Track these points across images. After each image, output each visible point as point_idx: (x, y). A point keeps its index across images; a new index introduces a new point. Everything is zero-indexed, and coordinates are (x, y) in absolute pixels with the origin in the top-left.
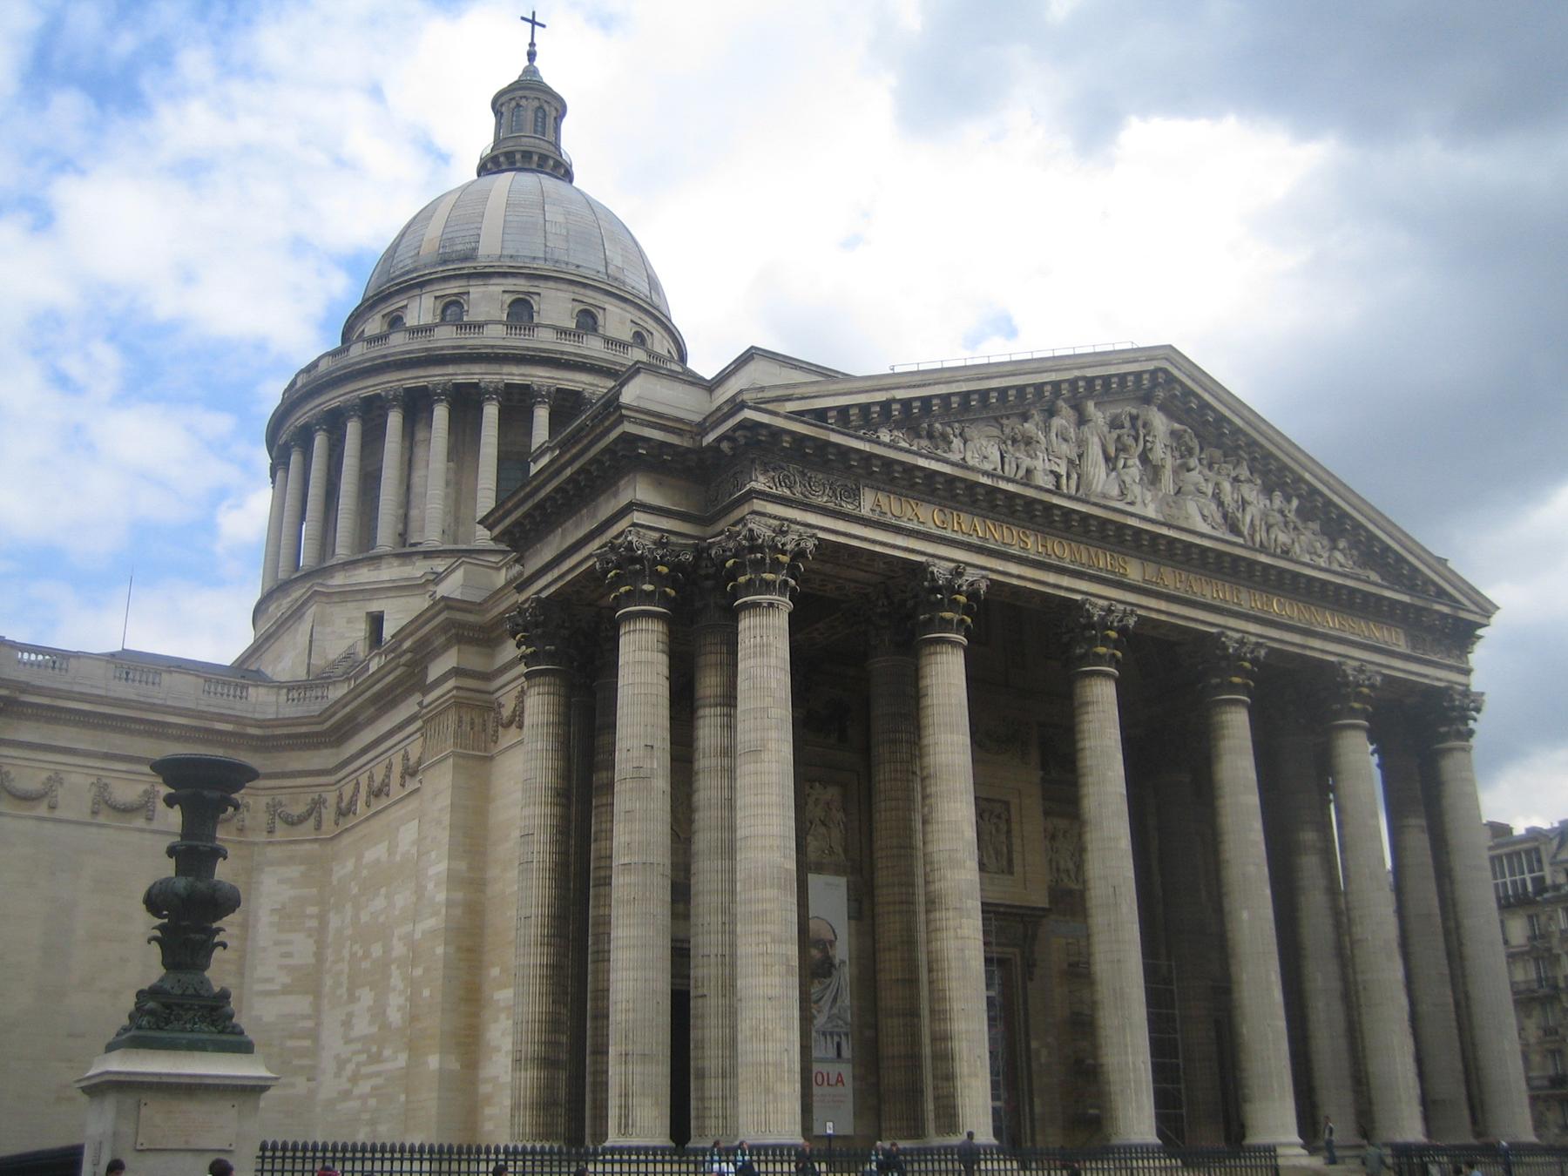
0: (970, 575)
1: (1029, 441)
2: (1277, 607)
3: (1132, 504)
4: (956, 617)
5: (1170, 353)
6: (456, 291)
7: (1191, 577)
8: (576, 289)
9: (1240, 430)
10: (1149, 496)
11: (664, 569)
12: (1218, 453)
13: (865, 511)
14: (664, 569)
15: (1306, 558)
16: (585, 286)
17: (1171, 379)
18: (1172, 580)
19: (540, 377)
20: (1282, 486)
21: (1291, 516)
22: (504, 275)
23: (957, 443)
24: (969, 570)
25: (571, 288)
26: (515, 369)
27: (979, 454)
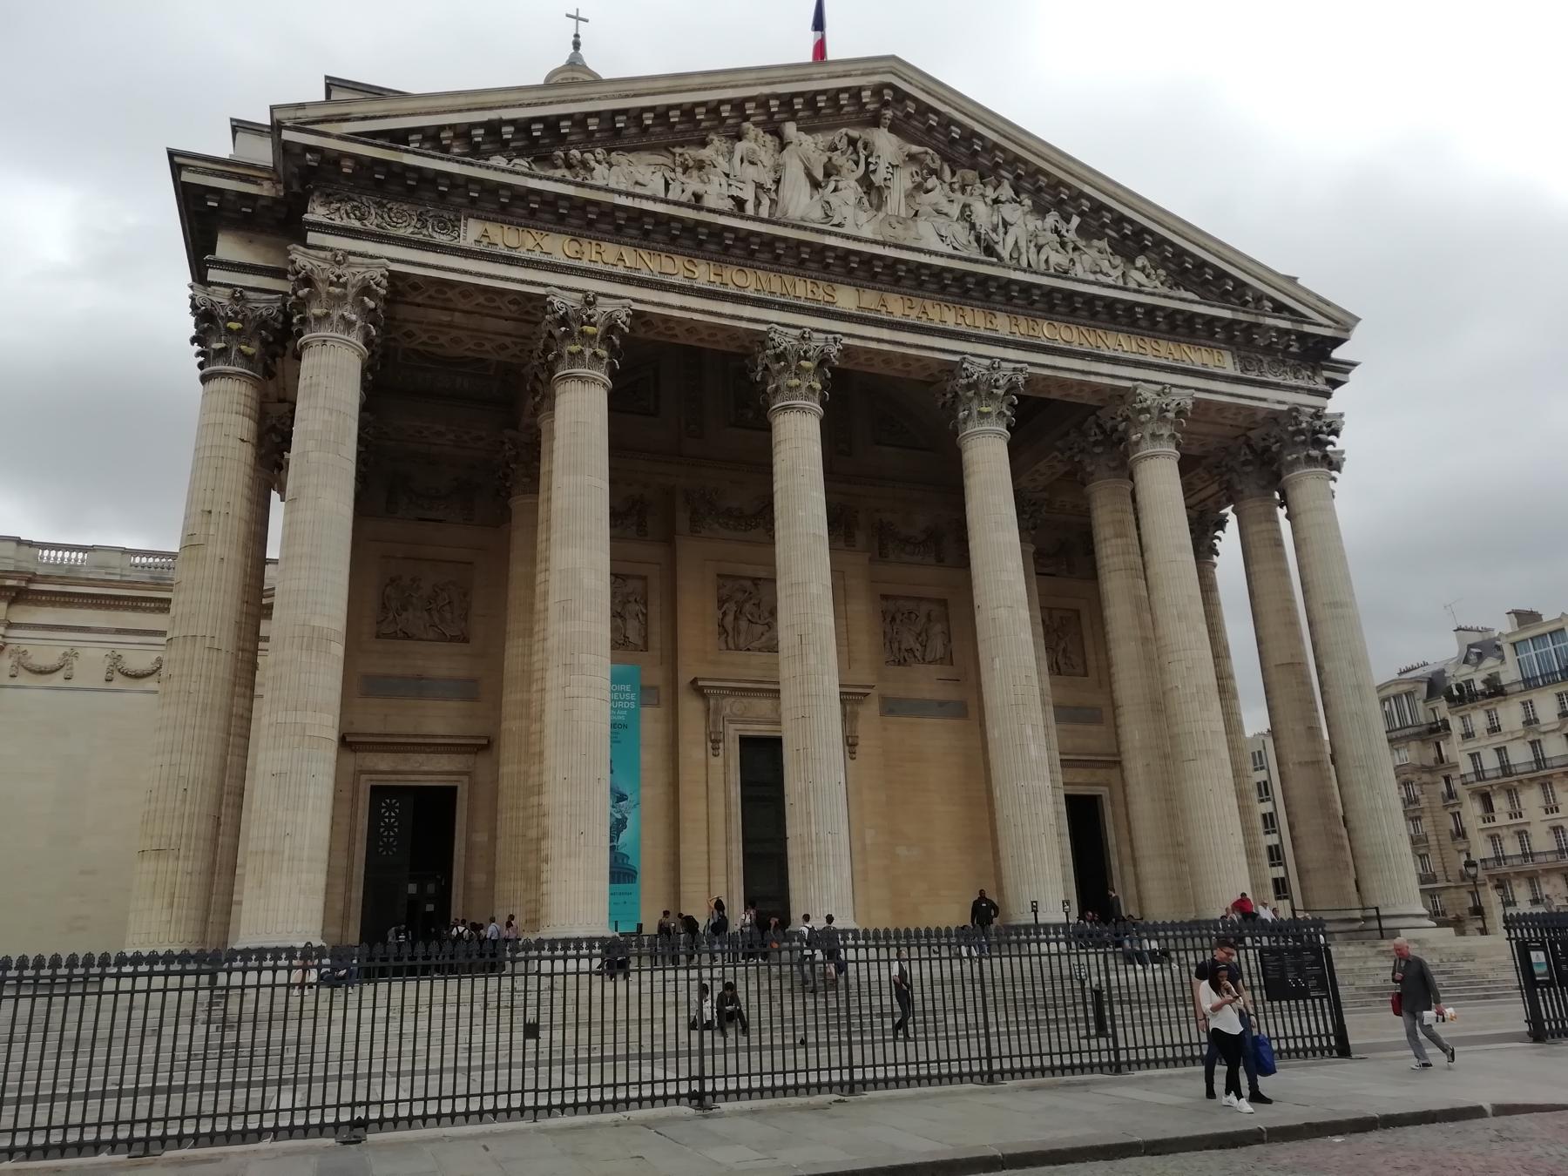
0: (604, 307)
1: (700, 165)
2: (1046, 332)
3: (838, 225)
4: (588, 352)
5: (893, 63)
7: (928, 303)
9: (996, 146)
10: (863, 217)
12: (971, 175)
14: (235, 326)
15: (1092, 277)
17: (901, 97)
18: (896, 307)
20: (1059, 205)
21: (1071, 236)
23: (600, 170)
24: (601, 300)
27: (632, 178)
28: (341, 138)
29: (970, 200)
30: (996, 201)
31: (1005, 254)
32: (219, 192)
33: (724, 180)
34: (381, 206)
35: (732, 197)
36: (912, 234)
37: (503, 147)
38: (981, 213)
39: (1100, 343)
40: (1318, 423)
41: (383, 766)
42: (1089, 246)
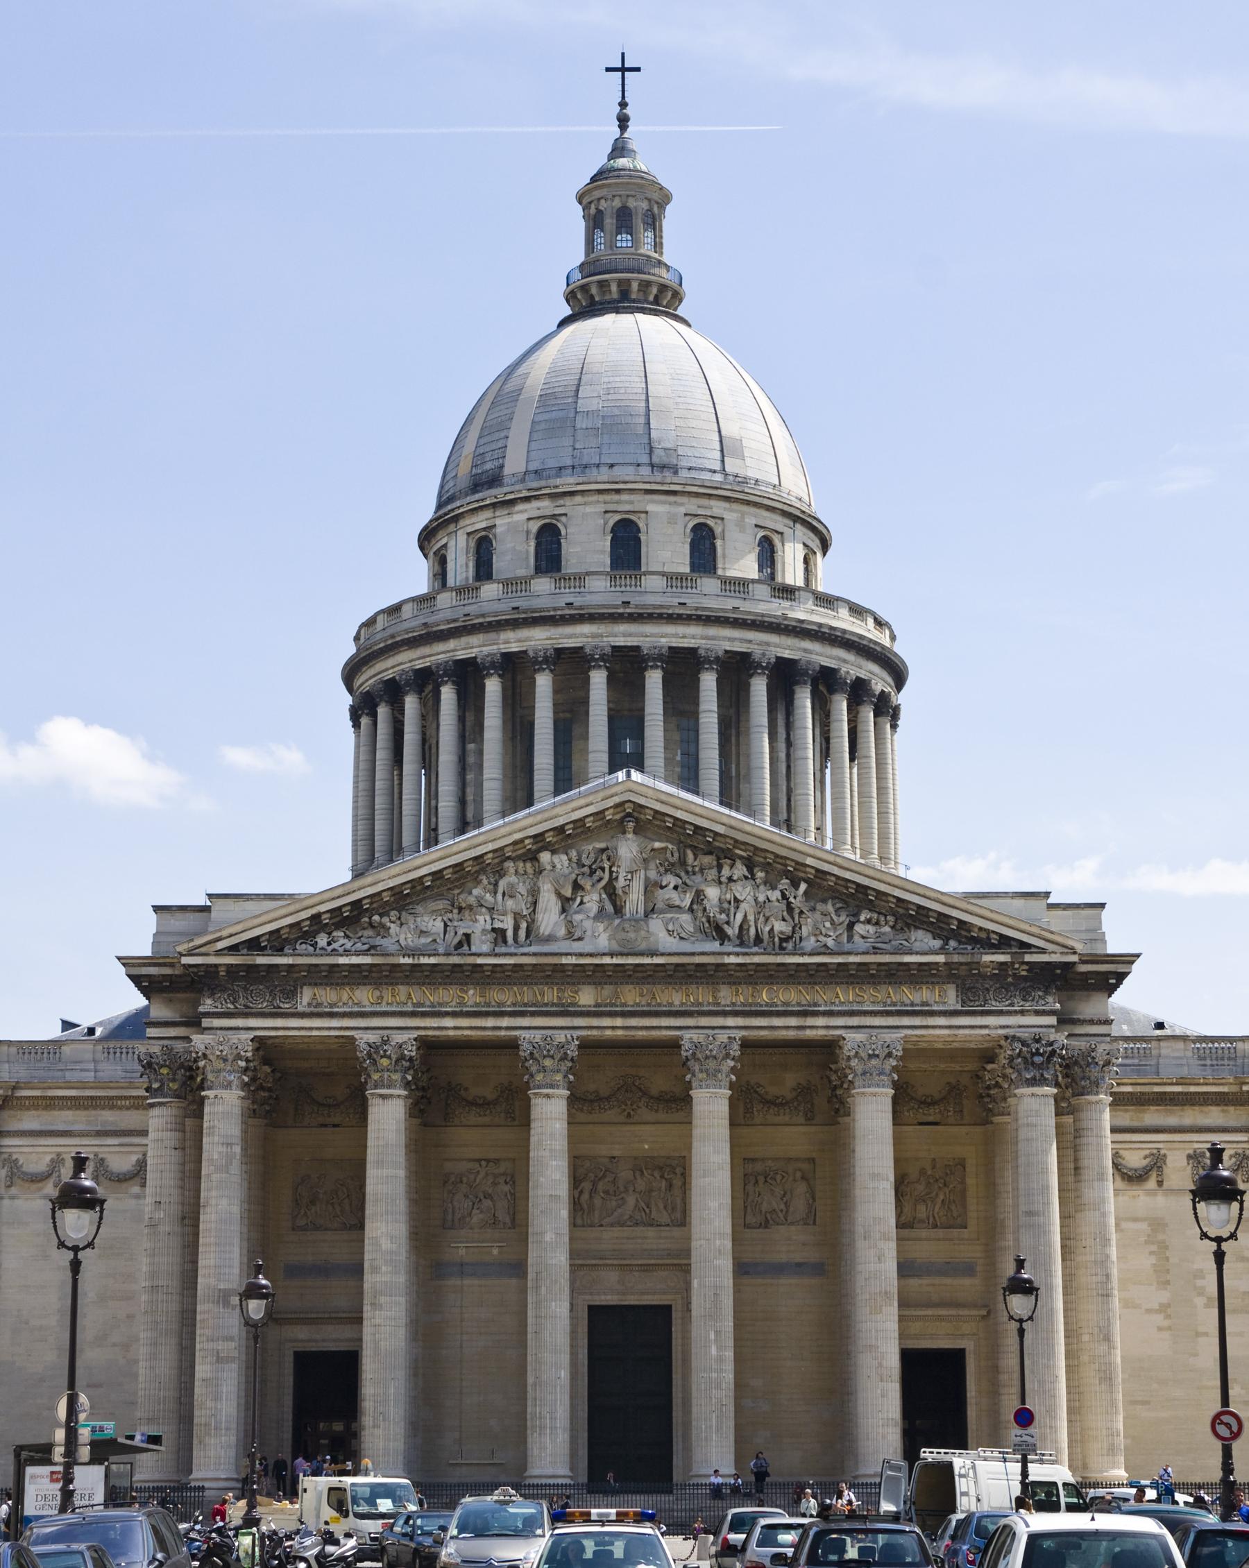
0: (399, 1038)
1: (470, 907)
3: (580, 939)
6: (483, 525)
7: (657, 989)
8: (607, 497)
10: (601, 927)
11: (164, 1071)
12: (707, 860)
13: (300, 1009)
16: (618, 491)
18: (631, 996)
19: (538, 639)
20: (787, 874)
22: (527, 499)
23: (394, 928)
25: (601, 498)
26: (510, 635)
28: (219, 953)
29: (703, 887)
30: (730, 879)
31: (732, 931)
32: (148, 977)
33: (488, 918)
34: (246, 989)
35: (494, 930)
36: (643, 933)
37: (327, 929)
38: (712, 893)
39: (818, 999)
40: (1035, 1046)
41: (301, 1336)
42: (813, 909)
